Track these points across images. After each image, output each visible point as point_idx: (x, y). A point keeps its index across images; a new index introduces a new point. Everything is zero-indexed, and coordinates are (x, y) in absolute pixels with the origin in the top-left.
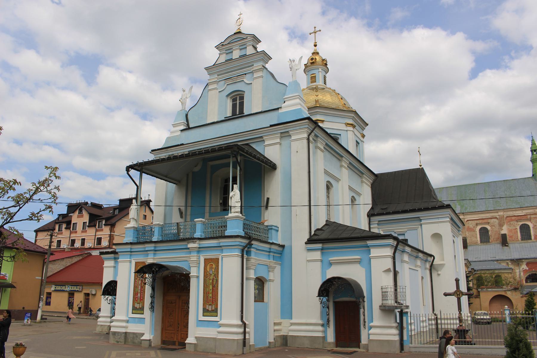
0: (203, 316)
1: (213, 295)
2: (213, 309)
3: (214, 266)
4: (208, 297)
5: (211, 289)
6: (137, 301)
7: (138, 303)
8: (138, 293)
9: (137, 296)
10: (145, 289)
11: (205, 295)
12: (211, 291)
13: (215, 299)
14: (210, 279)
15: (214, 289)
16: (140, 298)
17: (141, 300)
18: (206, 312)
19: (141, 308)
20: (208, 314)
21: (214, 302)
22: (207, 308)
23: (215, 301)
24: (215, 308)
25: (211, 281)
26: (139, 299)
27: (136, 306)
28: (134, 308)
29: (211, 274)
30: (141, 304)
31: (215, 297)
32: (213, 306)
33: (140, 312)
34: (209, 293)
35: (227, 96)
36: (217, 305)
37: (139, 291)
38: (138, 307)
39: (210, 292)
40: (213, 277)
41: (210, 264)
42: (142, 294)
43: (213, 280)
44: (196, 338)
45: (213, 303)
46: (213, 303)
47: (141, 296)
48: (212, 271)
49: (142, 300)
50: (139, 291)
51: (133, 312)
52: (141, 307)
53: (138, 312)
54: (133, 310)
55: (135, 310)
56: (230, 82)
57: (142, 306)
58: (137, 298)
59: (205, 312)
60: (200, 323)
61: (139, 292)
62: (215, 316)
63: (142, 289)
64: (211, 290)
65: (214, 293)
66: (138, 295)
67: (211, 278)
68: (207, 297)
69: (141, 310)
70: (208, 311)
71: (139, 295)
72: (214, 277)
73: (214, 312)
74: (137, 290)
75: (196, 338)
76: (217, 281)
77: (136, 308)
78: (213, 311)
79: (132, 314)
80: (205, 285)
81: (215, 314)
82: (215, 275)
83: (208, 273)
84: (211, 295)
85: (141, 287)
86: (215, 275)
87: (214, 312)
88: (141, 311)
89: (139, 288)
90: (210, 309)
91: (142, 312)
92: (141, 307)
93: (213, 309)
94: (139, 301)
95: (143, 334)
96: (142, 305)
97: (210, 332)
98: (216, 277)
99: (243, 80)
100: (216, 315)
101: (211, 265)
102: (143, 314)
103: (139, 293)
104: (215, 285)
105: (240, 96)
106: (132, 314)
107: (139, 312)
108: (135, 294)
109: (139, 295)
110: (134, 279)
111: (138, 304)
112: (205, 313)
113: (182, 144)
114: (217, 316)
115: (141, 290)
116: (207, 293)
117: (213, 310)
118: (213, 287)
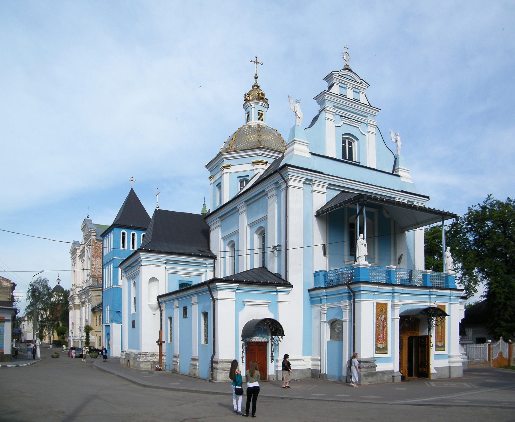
0: (436, 351)
1: (441, 334)
2: (442, 345)
6: (380, 341)
7: (380, 344)
8: (380, 333)
12: (440, 331)
16: (383, 339)
17: (383, 340)
19: (384, 348)
20: (439, 349)
22: (438, 345)
24: (443, 344)
26: (382, 340)
27: (379, 346)
28: (377, 349)
30: (384, 344)
32: (442, 343)
33: (384, 352)
37: (381, 332)
38: (381, 348)
45: (442, 340)
46: (442, 340)
47: (383, 336)
49: (385, 340)
50: (381, 332)
51: (377, 352)
52: (384, 347)
53: (382, 352)
54: (376, 350)
55: (378, 350)
57: (385, 346)
58: (380, 338)
59: (437, 348)
60: (437, 357)
61: (382, 333)
66: (380, 335)
69: (384, 350)
71: (381, 335)
74: (379, 330)
78: (442, 346)
79: (376, 354)
81: (443, 349)
84: (440, 334)
89: (381, 329)
90: (440, 346)
92: (384, 347)
93: (442, 345)
94: (381, 341)
95: (392, 371)
97: (444, 363)
100: (444, 350)
103: (381, 334)
105: (349, 140)
106: (376, 354)
108: (378, 334)
109: (381, 335)
111: (381, 345)
113: (322, 173)
114: (445, 350)
115: (383, 331)
116: (437, 333)
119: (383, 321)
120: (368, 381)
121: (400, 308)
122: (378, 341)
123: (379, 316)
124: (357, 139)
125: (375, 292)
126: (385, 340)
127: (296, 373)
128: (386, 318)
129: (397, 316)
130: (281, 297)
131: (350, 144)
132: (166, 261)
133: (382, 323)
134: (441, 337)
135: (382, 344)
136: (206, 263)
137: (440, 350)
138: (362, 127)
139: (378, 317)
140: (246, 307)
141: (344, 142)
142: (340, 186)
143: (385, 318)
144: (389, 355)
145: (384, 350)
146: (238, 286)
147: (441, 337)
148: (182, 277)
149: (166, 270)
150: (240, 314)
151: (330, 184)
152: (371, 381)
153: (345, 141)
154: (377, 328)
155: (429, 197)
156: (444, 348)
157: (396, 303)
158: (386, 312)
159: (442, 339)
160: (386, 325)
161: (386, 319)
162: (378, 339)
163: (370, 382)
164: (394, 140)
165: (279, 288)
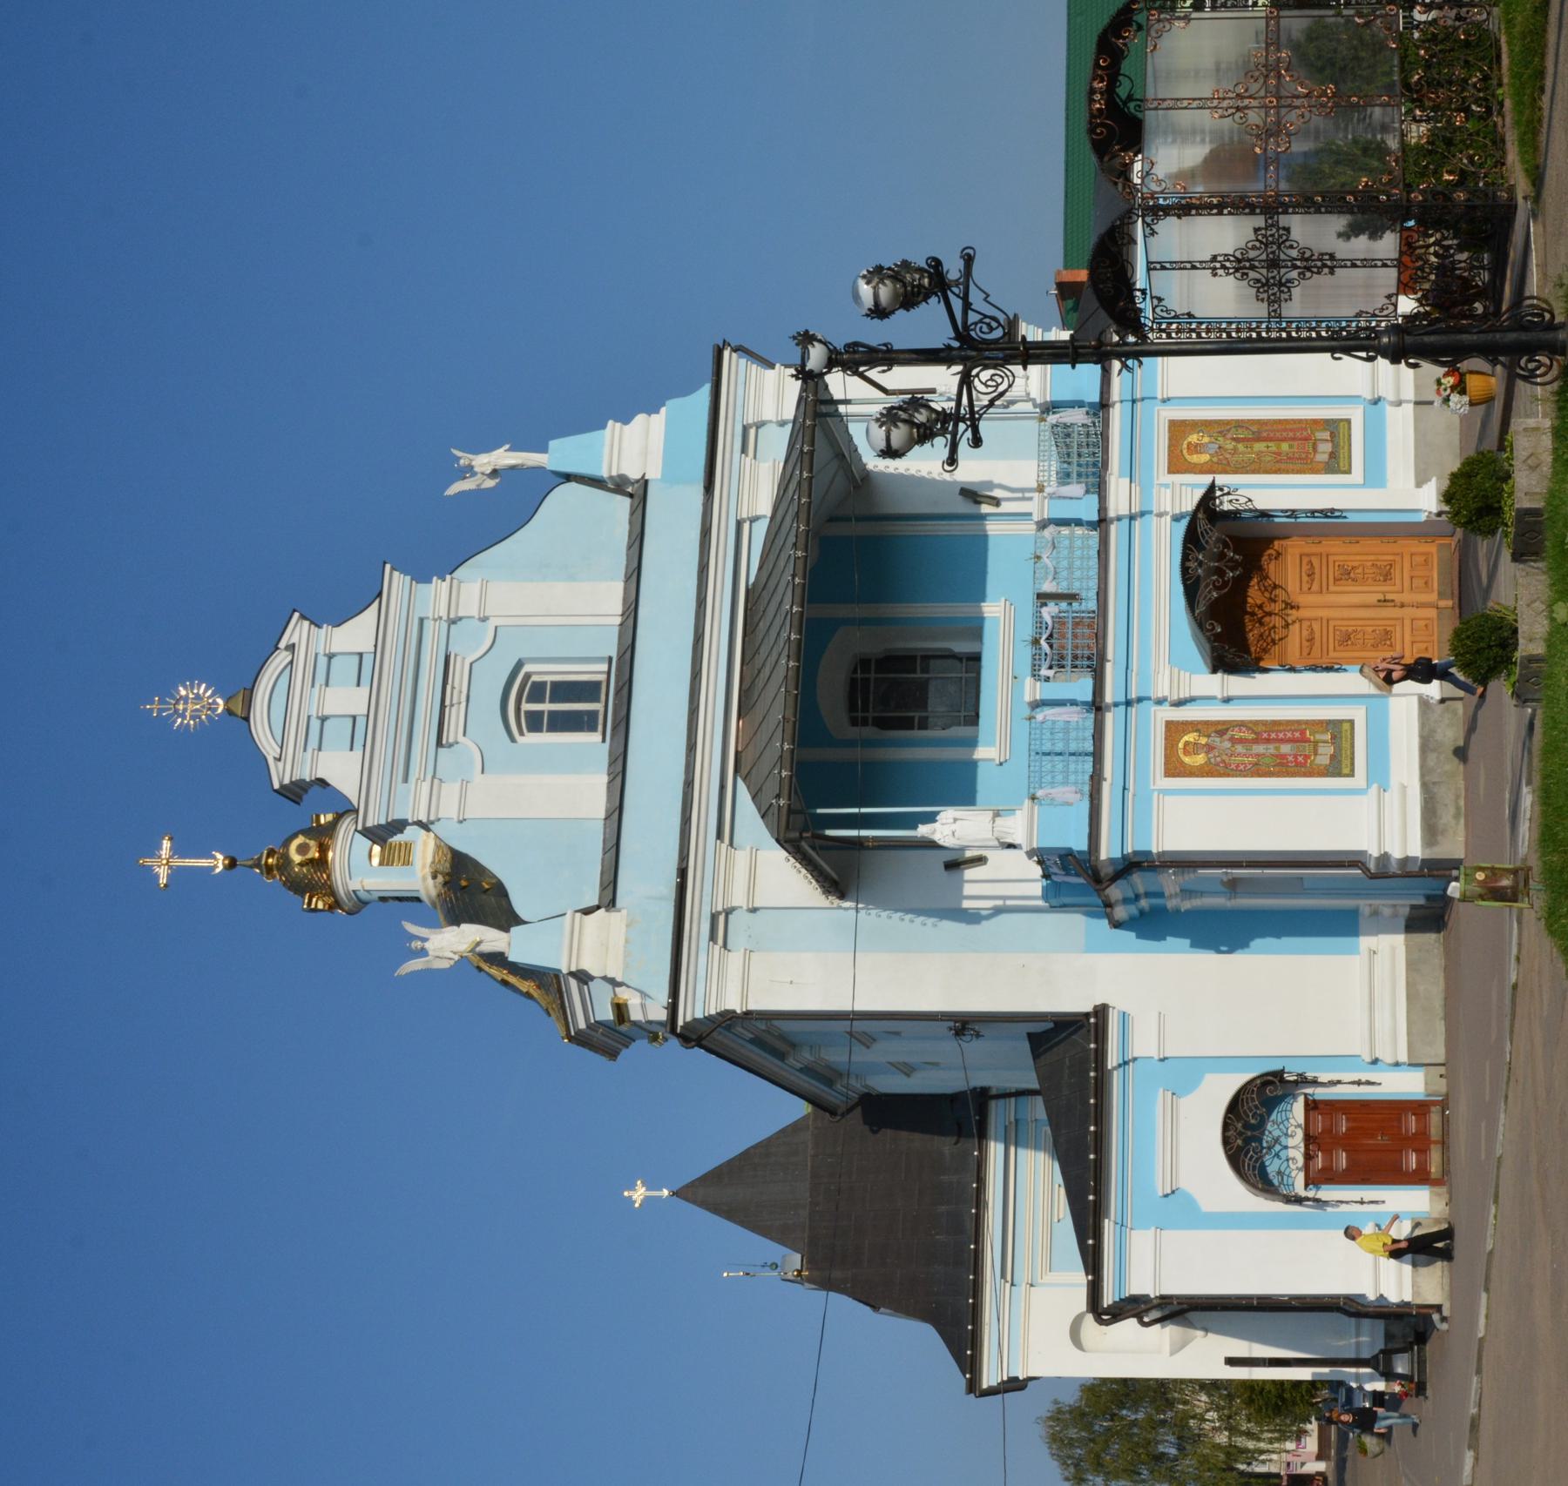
1: (1284, 440)
2: (1326, 435)
3: (1193, 438)
4: (1291, 455)
5: (1264, 444)
6: (1306, 757)
8: (1277, 756)
9: (1290, 758)
10: (1264, 723)
11: (1283, 466)
12: (1273, 446)
13: (1298, 430)
14: (1235, 449)
15: (1265, 434)
18: (1337, 463)
19: (1333, 737)
20: (1342, 453)
21: (1305, 433)
23: (1302, 429)
25: (1241, 447)
27: (1323, 759)
29: (1220, 447)
30: (1319, 737)
31: (1291, 430)
34: (1279, 454)
35: (513, 740)
36: (1315, 422)
38: (1331, 750)
39: (1274, 449)
40: (1228, 442)
41: (1185, 452)
42: (1281, 736)
43: (1237, 440)
44: (1419, 484)
45: (1306, 439)
46: (1306, 439)
48: (1210, 445)
49: (1303, 732)
50: (1271, 749)
52: (1328, 737)
53: (1345, 745)
54: (1339, 774)
56: (455, 718)
58: (1295, 756)
62: (1350, 428)
63: (1265, 735)
64: (1268, 447)
65: (1278, 434)
66: (1283, 756)
67: (1230, 445)
68: (1289, 458)
69: (1339, 731)
70: (1333, 455)
71: (1286, 749)
72: (1229, 436)
73: (1337, 430)
74: (1267, 760)
75: (1419, 484)
76: (1239, 424)
77: (1333, 757)
79: (1353, 776)
80: (1253, 467)
82: (1219, 432)
83: (1215, 459)
84: (1285, 446)
85: (1256, 741)
86: (1219, 432)
87: (1337, 430)
88: (1341, 732)
89: (1259, 749)
91: (1346, 726)
93: (1326, 435)
94: (1308, 748)
96: (1323, 733)
98: (1229, 431)
99: (471, 664)
101: (1188, 448)
102: (1352, 722)
103: (1277, 749)
104: (1253, 433)
106: (1353, 776)
107: (1346, 741)
110: (1228, 776)
111: (1320, 752)
112: (1341, 464)
114: (1349, 421)
115: (1268, 741)
117: (1332, 433)
118: (1259, 439)
119: (1233, 740)
120: (1453, 822)
121: (1182, 673)
122: (1304, 765)
123: (1212, 760)
124: (519, 665)
125: (1124, 789)
126: (1298, 732)
127: (1421, 988)
128: (1220, 727)
129: (1216, 684)
130: (1144, 1044)
131: (537, 692)
132: (1008, 1285)
133: (1240, 748)
134: (1295, 443)
135: (1316, 743)
136: (1006, 1127)
137: (1346, 448)
138: (467, 651)
139: (1218, 765)
140: (1184, 1183)
141: (535, 723)
142: (722, 787)
143: (1221, 733)
144: (1357, 714)
145: (1341, 738)
146: (1112, 1223)
147: (1294, 439)
148: (1061, 1217)
149: (1040, 1281)
150: (1207, 1205)
151: (719, 835)
152: (1452, 810)
153: (530, 714)
154: (1257, 771)
155: (718, 346)
156: (1342, 424)
157: (1163, 688)
158: (1200, 727)
159: (1305, 433)
160: (1249, 729)
161: (1222, 728)
162: (1297, 764)
163: (1457, 816)
164: (490, 483)
165: (1112, 1060)
